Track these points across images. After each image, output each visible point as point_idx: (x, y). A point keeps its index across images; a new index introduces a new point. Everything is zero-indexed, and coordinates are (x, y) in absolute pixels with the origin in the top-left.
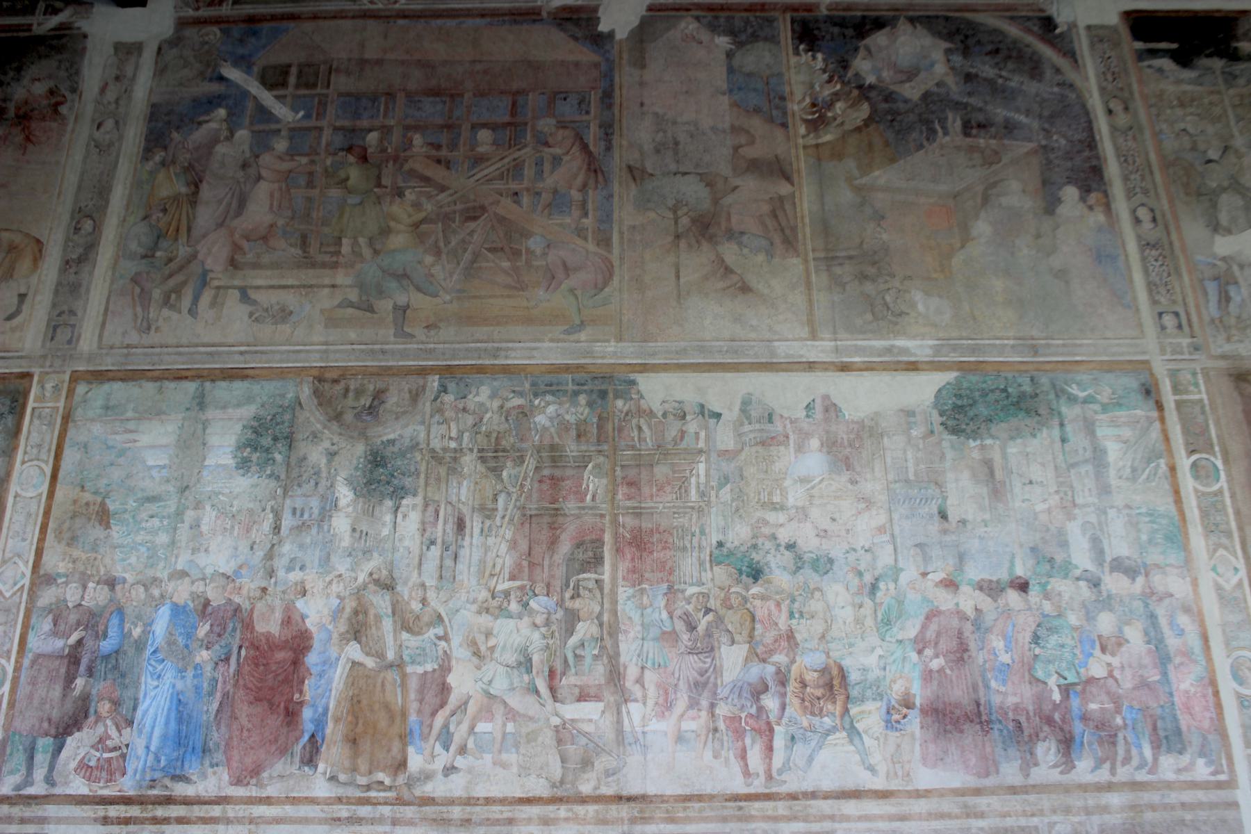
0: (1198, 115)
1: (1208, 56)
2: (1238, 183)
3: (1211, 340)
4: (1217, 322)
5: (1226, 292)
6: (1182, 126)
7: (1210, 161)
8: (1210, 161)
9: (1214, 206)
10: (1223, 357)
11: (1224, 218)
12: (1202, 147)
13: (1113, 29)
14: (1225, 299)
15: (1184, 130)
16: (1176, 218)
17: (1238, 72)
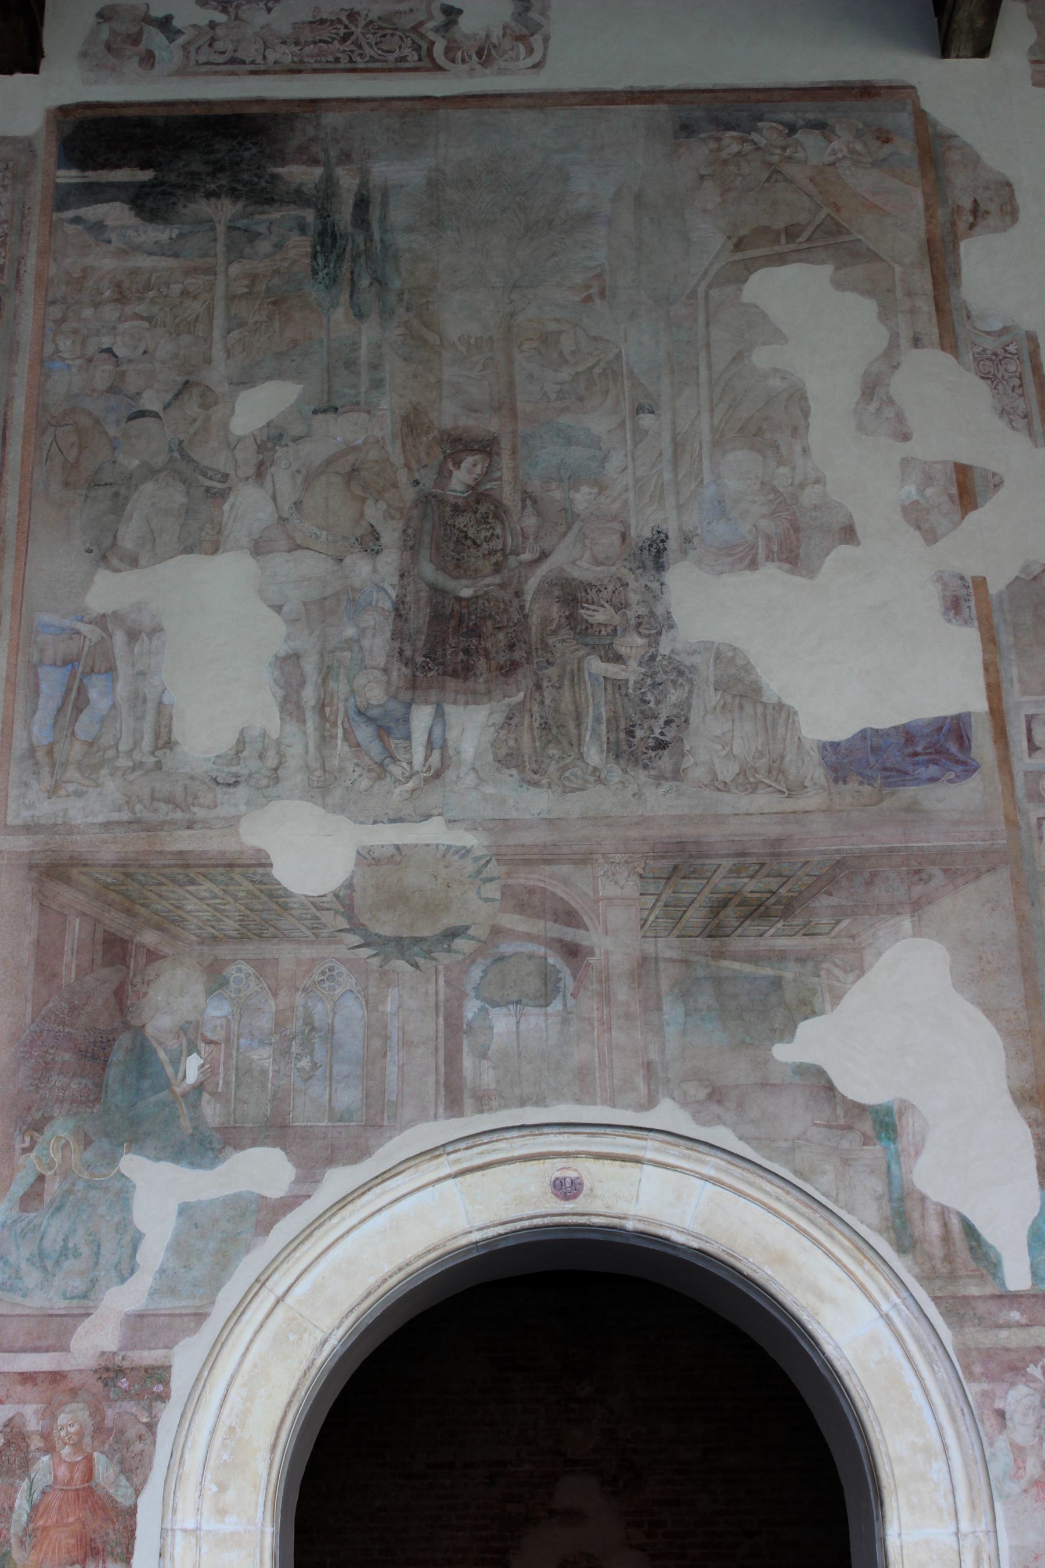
0: (149, 319)
1: (209, 195)
2: (186, 457)
3: (13, 792)
4: (40, 755)
5: (82, 690)
6: (106, 342)
7: (142, 414)
8: (142, 414)
9: (118, 506)
10: (28, 829)
11: (129, 536)
12: (132, 383)
13: (27, 145)
14: (76, 701)
15: (109, 351)
16: (25, 535)
17: (262, 229)
